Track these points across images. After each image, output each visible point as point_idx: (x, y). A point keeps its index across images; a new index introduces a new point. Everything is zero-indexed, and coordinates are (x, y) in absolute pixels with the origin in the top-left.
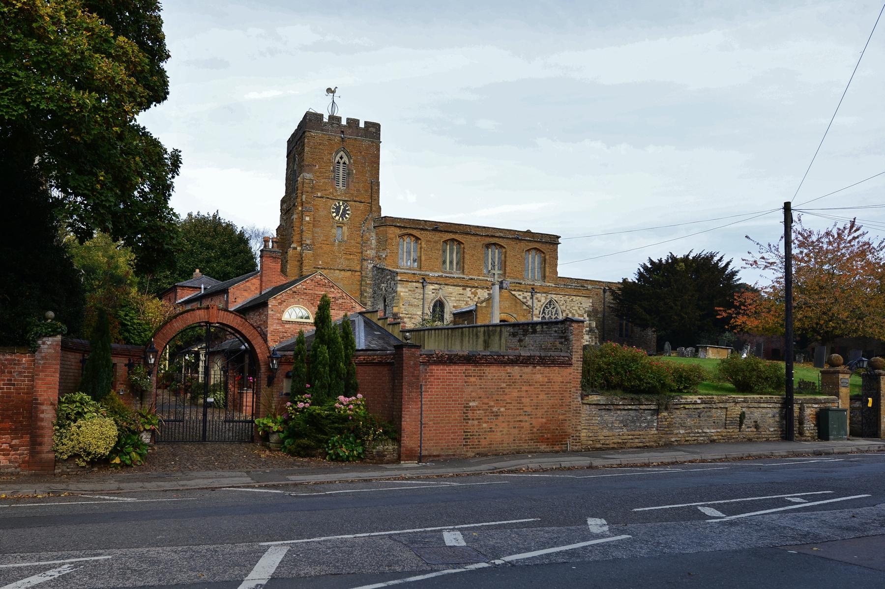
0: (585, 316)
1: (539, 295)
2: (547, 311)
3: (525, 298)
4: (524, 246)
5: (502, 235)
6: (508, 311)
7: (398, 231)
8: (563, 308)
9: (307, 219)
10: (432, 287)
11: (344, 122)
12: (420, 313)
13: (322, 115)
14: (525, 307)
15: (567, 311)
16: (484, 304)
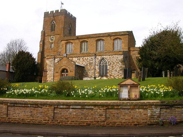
0: (120, 63)
1: (98, 57)
2: (102, 63)
3: (92, 58)
4: (112, 38)
5: (102, 35)
6: (66, 65)
7: (66, 42)
8: (109, 61)
9: (41, 43)
10: (57, 59)
11: (54, 12)
12: (53, 69)
13: (49, 12)
14: (72, 63)
15: (111, 62)
16: (57, 64)
